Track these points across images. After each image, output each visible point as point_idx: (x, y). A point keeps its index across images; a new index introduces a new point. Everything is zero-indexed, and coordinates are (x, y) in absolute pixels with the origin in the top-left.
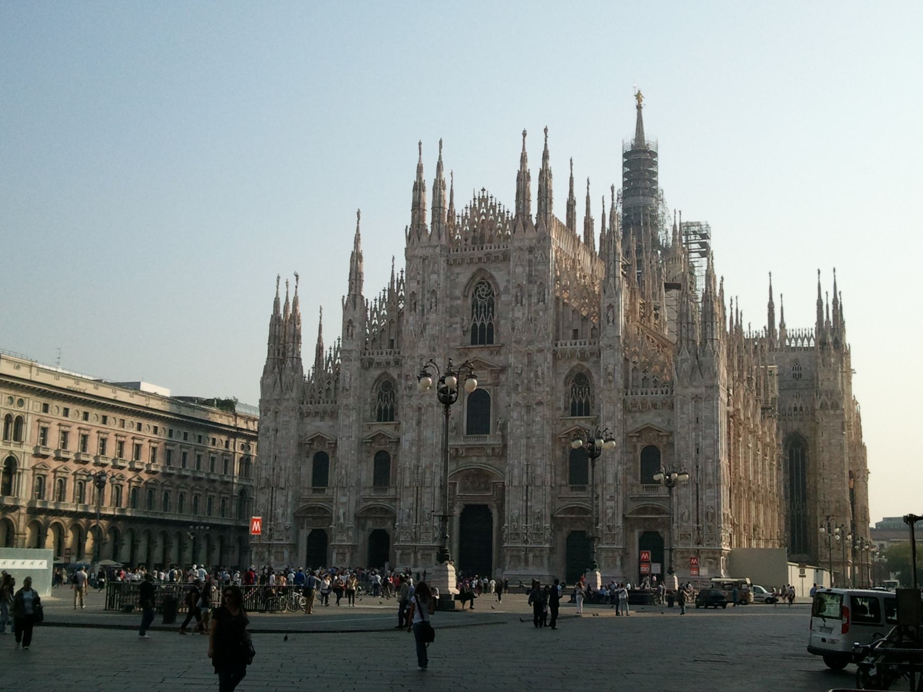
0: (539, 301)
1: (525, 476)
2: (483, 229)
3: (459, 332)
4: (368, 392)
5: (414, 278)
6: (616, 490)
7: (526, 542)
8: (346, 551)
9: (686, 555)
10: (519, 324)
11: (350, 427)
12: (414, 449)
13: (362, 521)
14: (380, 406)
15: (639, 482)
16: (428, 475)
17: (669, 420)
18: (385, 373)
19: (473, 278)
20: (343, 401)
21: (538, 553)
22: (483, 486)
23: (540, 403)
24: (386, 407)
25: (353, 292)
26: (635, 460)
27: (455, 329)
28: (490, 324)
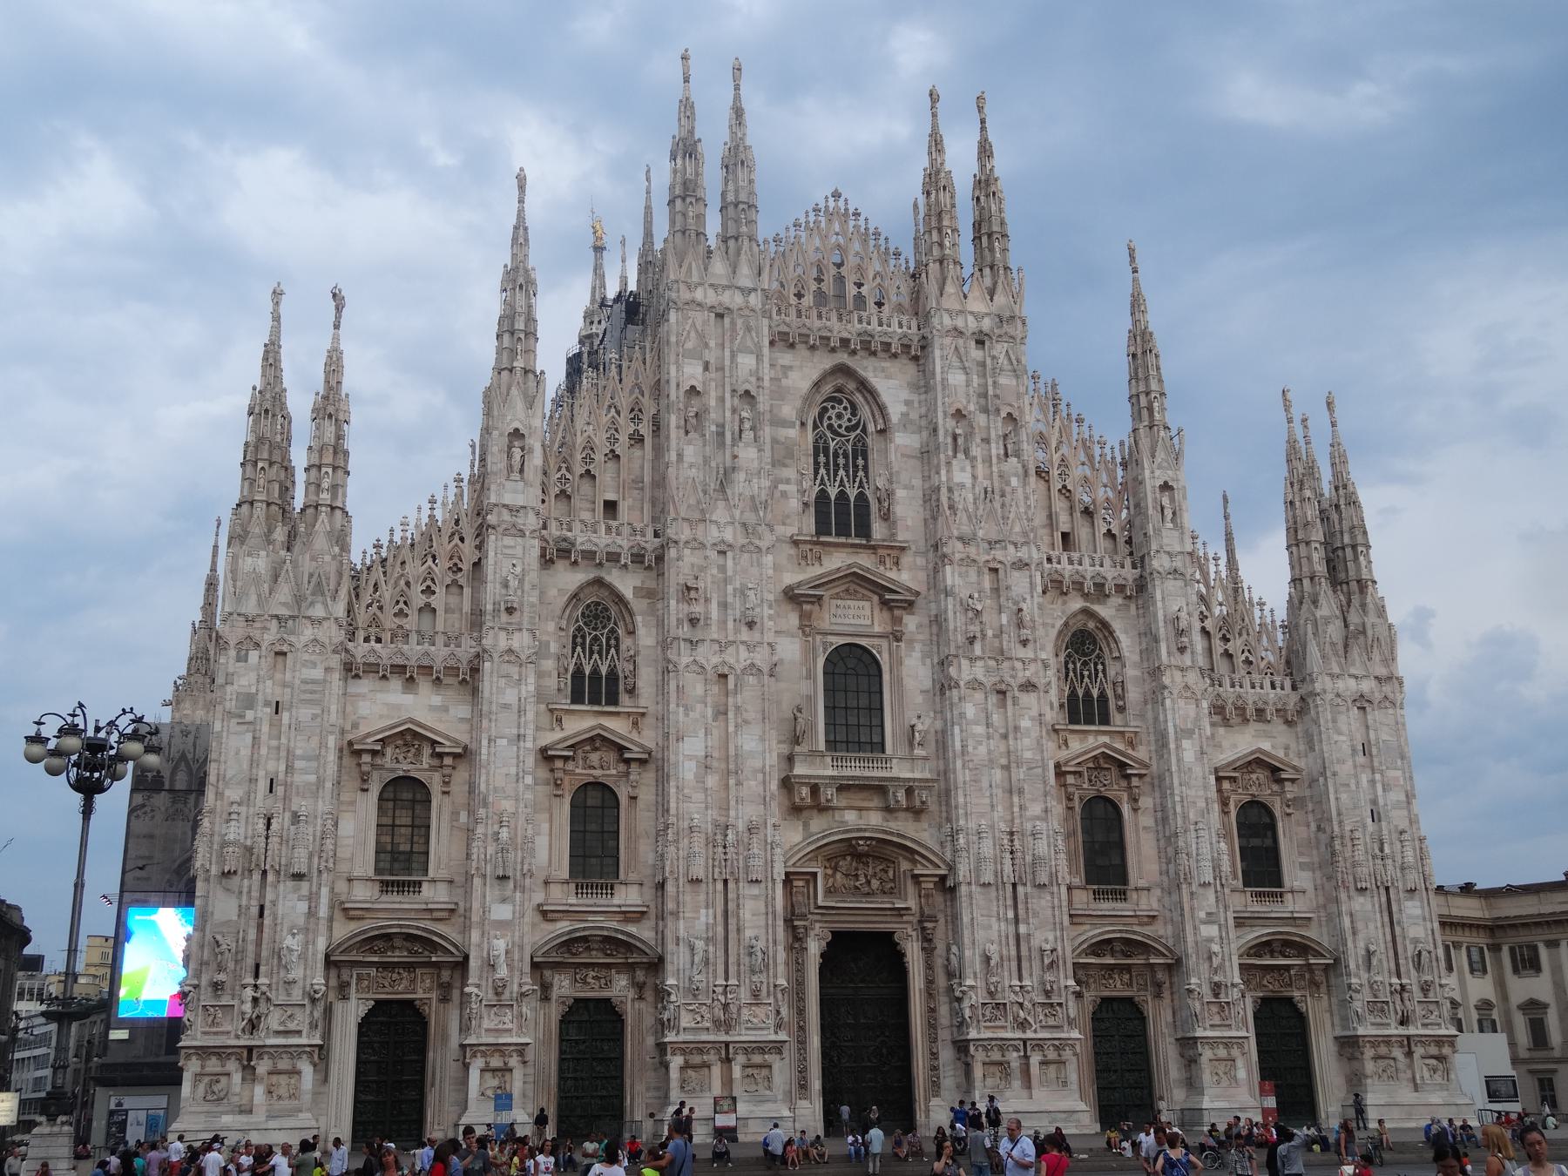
0: (1006, 455)
1: (1008, 856)
2: (840, 279)
3: (794, 504)
4: (551, 626)
5: (693, 355)
7: (1023, 1025)
8: (514, 1061)
9: (1383, 1050)
11: (521, 711)
12: (712, 781)
13: (547, 973)
15: (1240, 883)
17: (1287, 748)
19: (817, 385)
20: (497, 641)
21: (1052, 1055)
22: (875, 883)
23: (1029, 686)
25: (519, 364)
26: (1226, 836)
27: (784, 494)
28: (861, 497)
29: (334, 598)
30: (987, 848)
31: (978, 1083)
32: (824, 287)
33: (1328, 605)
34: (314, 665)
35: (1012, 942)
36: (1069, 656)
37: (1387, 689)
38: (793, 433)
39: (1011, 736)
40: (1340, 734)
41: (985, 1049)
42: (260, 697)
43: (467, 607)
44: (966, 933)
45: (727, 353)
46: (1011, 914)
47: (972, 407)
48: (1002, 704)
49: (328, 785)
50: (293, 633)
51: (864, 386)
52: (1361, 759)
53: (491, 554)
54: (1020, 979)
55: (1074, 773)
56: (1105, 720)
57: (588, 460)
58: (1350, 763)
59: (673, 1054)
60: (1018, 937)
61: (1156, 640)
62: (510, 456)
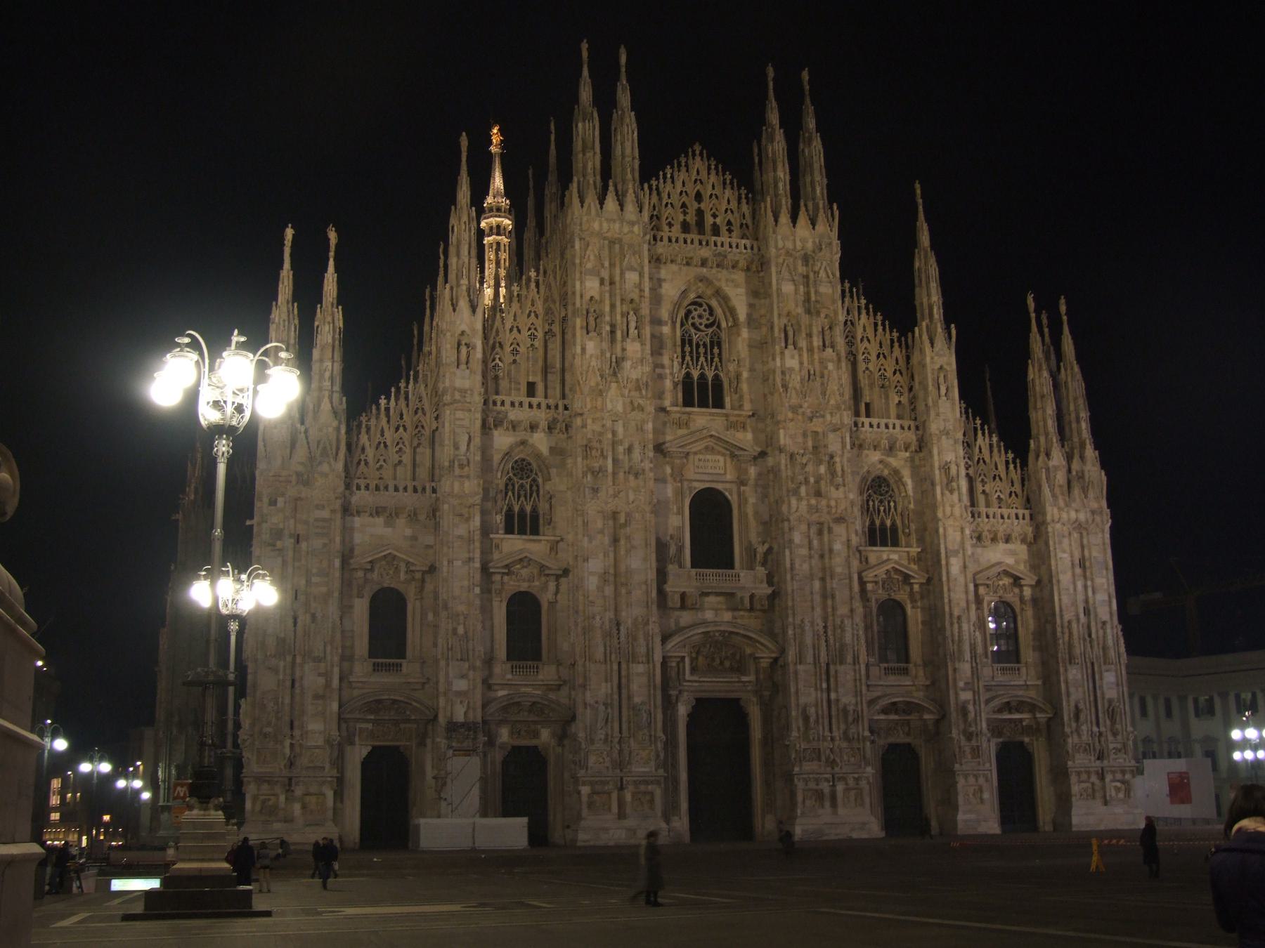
0: (824, 346)
1: (824, 644)
3: (668, 384)
5: (595, 272)
6: (975, 671)
7: (832, 763)
10: (795, 381)
11: (470, 540)
12: (609, 590)
14: (510, 510)
16: (641, 641)
18: (523, 443)
22: (727, 664)
23: (840, 520)
24: (522, 510)
25: (464, 282)
28: (716, 377)
29: (336, 460)
30: (809, 640)
31: (800, 805)
32: (688, 218)
33: (1057, 458)
34: (323, 507)
35: (825, 704)
36: (870, 496)
37: (1098, 518)
38: (666, 330)
39: (827, 556)
40: (1064, 552)
41: (804, 779)
42: (286, 532)
43: (428, 464)
44: (793, 699)
45: (618, 271)
46: (824, 685)
47: (800, 310)
48: (820, 533)
49: (336, 594)
50: (307, 483)
51: (718, 293)
52: (1078, 571)
53: (447, 425)
54: (831, 730)
55: (876, 583)
56: (895, 543)
57: (515, 352)
58: (1069, 573)
59: (584, 784)
60: (829, 701)
61: (933, 484)
62: (458, 352)
